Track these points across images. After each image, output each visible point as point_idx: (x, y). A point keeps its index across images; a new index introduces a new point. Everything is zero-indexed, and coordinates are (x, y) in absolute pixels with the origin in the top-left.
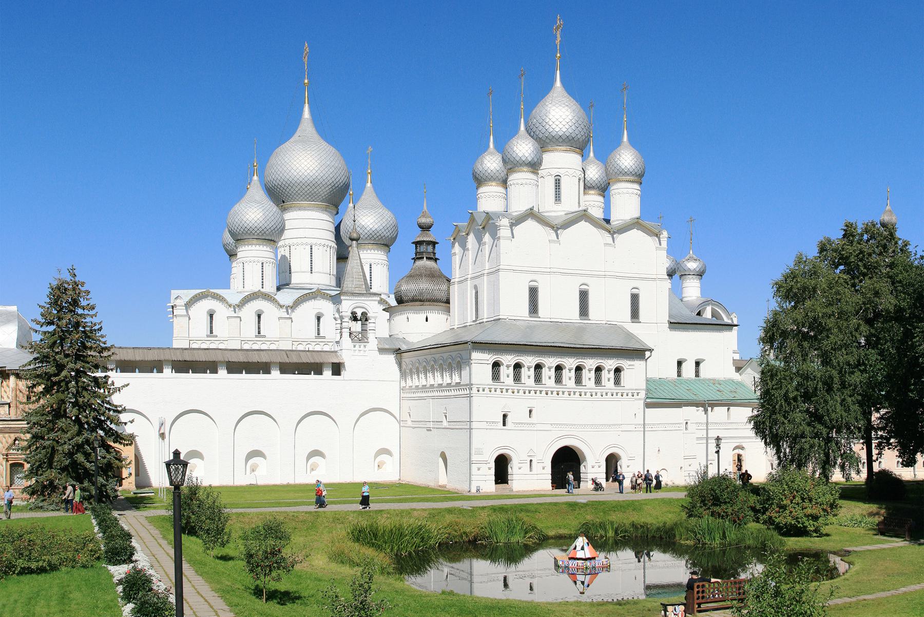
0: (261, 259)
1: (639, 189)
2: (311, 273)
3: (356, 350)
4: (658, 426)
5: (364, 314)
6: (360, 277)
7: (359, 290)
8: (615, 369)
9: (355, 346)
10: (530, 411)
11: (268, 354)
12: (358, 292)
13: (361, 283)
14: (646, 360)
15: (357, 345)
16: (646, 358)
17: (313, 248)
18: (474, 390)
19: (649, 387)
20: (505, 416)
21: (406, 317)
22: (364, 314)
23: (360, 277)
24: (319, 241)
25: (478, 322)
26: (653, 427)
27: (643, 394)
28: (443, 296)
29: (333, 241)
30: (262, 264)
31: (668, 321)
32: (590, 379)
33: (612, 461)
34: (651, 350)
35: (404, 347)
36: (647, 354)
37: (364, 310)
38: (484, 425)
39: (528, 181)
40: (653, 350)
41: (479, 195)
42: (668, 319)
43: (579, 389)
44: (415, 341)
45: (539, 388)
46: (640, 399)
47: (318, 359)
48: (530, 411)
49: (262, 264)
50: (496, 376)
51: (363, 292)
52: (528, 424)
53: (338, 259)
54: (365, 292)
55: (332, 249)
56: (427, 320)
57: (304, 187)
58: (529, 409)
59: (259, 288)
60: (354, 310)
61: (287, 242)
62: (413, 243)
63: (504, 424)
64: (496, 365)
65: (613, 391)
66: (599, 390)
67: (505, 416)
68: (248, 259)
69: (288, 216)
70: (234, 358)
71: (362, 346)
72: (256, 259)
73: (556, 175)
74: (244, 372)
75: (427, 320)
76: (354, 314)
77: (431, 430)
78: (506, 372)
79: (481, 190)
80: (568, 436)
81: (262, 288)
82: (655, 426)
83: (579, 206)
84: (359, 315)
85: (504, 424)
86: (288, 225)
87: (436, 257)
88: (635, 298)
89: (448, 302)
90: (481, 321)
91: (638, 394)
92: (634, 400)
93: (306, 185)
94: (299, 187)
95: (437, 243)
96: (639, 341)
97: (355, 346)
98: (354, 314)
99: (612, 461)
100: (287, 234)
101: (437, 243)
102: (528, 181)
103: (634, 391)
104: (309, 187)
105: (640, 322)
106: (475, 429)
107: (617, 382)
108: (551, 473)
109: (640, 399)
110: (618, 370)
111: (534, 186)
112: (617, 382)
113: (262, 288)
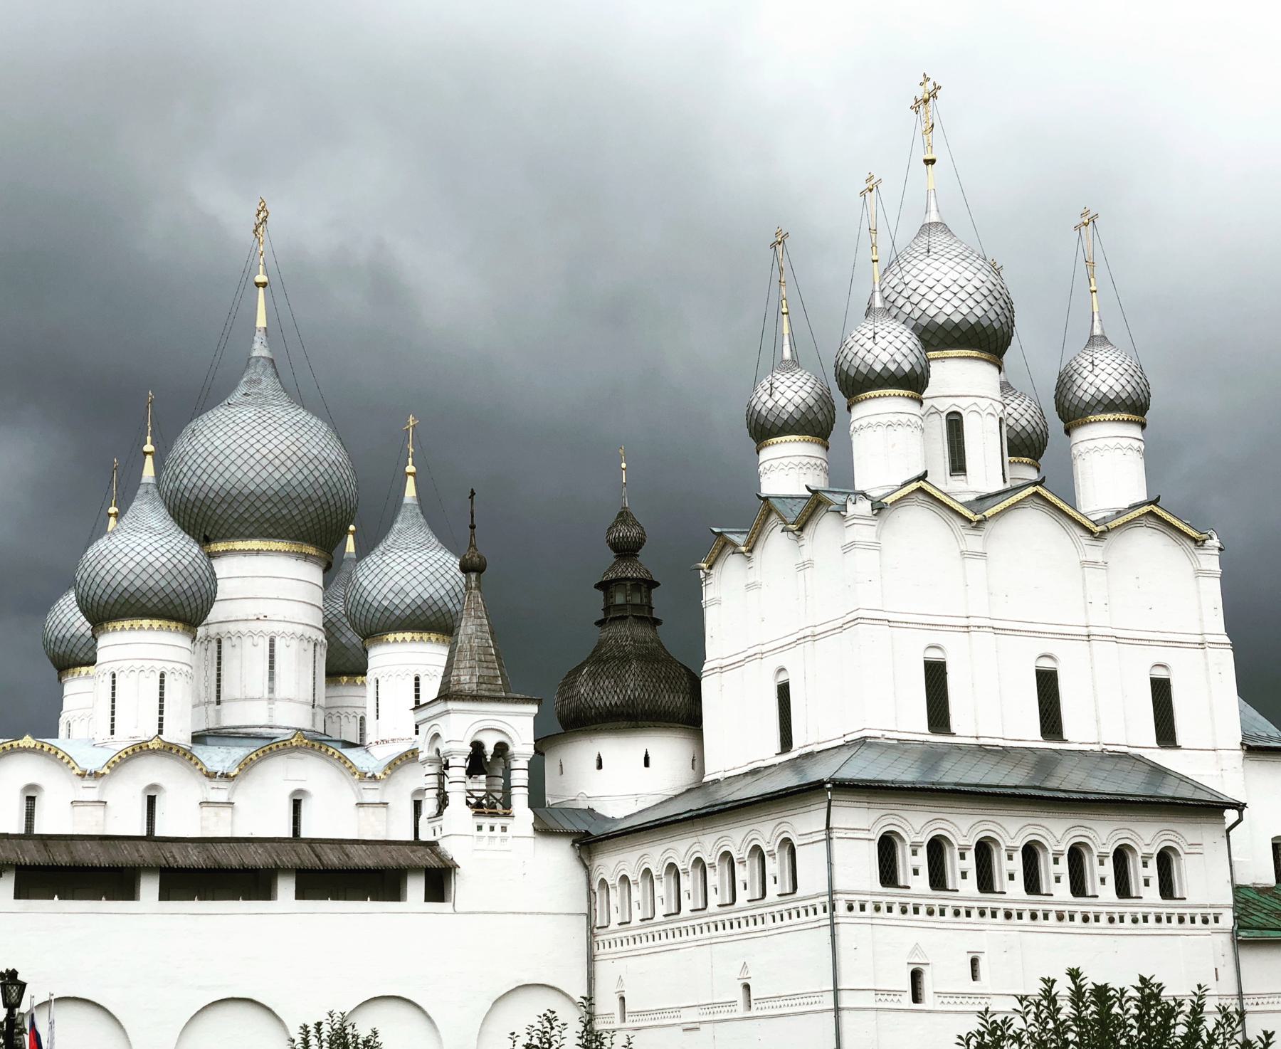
0: (159, 667)
1: (1142, 438)
3: (482, 837)
4: (1271, 1000)
5: (501, 749)
6: (489, 658)
7: (489, 690)
8: (1158, 854)
9: (480, 828)
10: (974, 962)
11: (266, 850)
12: (487, 694)
13: (491, 673)
14: (1228, 831)
15: (486, 822)
16: (1227, 826)
18: (841, 908)
19: (1236, 897)
20: (916, 976)
21: (596, 757)
22: (501, 749)
23: (489, 658)
24: (290, 628)
25: (793, 755)
26: (1260, 1001)
27: (1228, 920)
28: (680, 701)
29: (320, 629)
30: (162, 675)
31: (1242, 744)
32: (1103, 880)
34: (1240, 807)
35: (595, 831)
36: (1231, 815)
37: (500, 738)
38: (868, 1000)
39: (904, 418)
40: (1244, 805)
41: (767, 465)
42: (1240, 740)
43: (1081, 906)
44: (619, 814)
45: (988, 901)
46: (1222, 931)
48: (974, 962)
49: (162, 675)
50: (888, 875)
51: (497, 694)
52: (970, 995)
53: (328, 674)
54: (504, 694)
55: (318, 648)
56: (647, 764)
57: (258, 504)
58: (971, 956)
60: (481, 737)
61: (213, 630)
63: (916, 998)
64: (887, 847)
66: (1128, 908)
67: (916, 976)
68: (127, 664)
69: (223, 567)
70: (182, 858)
71: (497, 828)
72: (148, 664)
73: (955, 409)
75: (647, 764)
76: (477, 747)
77: (698, 1029)
78: (912, 864)
79: (765, 454)
82: (1265, 1001)
83: (1005, 481)
84: (489, 749)
85: (916, 998)
86: (224, 589)
88: (1161, 691)
90: (808, 750)
91: (1216, 920)
92: (1209, 932)
93: (264, 499)
94: (247, 504)
95: (656, 584)
96: (1198, 787)
97: (480, 828)
98: (477, 747)
100: (216, 613)
101: (656, 584)
102: (904, 418)
103: (1209, 911)
104: (269, 505)
105: (1179, 747)
106: (849, 1009)
107: (1167, 890)
109: (1222, 931)
110: (1165, 860)
111: (918, 432)
112: (1167, 890)
113: (160, 732)
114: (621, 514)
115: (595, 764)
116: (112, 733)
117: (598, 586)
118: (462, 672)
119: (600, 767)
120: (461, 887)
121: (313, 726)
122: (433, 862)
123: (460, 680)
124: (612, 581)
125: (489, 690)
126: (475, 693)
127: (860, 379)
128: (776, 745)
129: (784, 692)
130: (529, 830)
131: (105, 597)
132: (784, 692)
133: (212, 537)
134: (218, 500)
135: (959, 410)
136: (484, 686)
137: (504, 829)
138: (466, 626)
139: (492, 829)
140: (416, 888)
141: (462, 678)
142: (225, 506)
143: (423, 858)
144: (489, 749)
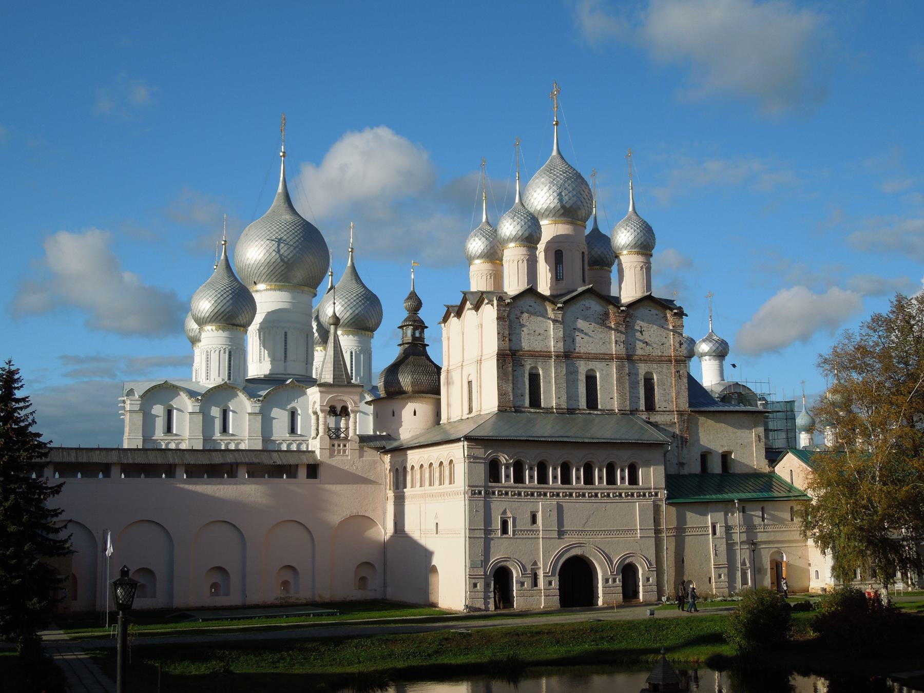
2: (285, 362)
7: (338, 381)
9: (333, 445)
11: (234, 456)
15: (336, 443)
17: (288, 334)
21: (392, 411)
33: (628, 572)
47: (292, 461)
51: (342, 384)
56: (415, 414)
59: (226, 380)
62: (399, 328)
65: (628, 491)
74: (205, 476)
75: (415, 414)
80: (580, 545)
81: (229, 379)
84: (339, 409)
87: (426, 343)
89: (437, 391)
95: (427, 327)
99: (628, 572)
101: (427, 327)
108: (558, 587)
112: (633, 480)
114: (410, 294)
115: (391, 414)
116: (208, 379)
117: (399, 328)
118: (327, 373)
119: (394, 415)
120: (322, 472)
121: (307, 373)
122: (311, 462)
123: (325, 377)
124: (405, 326)
125: (338, 381)
126: (332, 383)
127: (506, 238)
128: (466, 410)
129: (470, 383)
130: (357, 446)
131: (203, 315)
132: (470, 383)
133: (257, 283)
134: (259, 265)
135: (561, 249)
136: (336, 380)
137: (345, 446)
138: (329, 351)
139: (339, 446)
140: (302, 473)
141: (326, 376)
142: (262, 268)
143: (306, 460)
144: (339, 409)
